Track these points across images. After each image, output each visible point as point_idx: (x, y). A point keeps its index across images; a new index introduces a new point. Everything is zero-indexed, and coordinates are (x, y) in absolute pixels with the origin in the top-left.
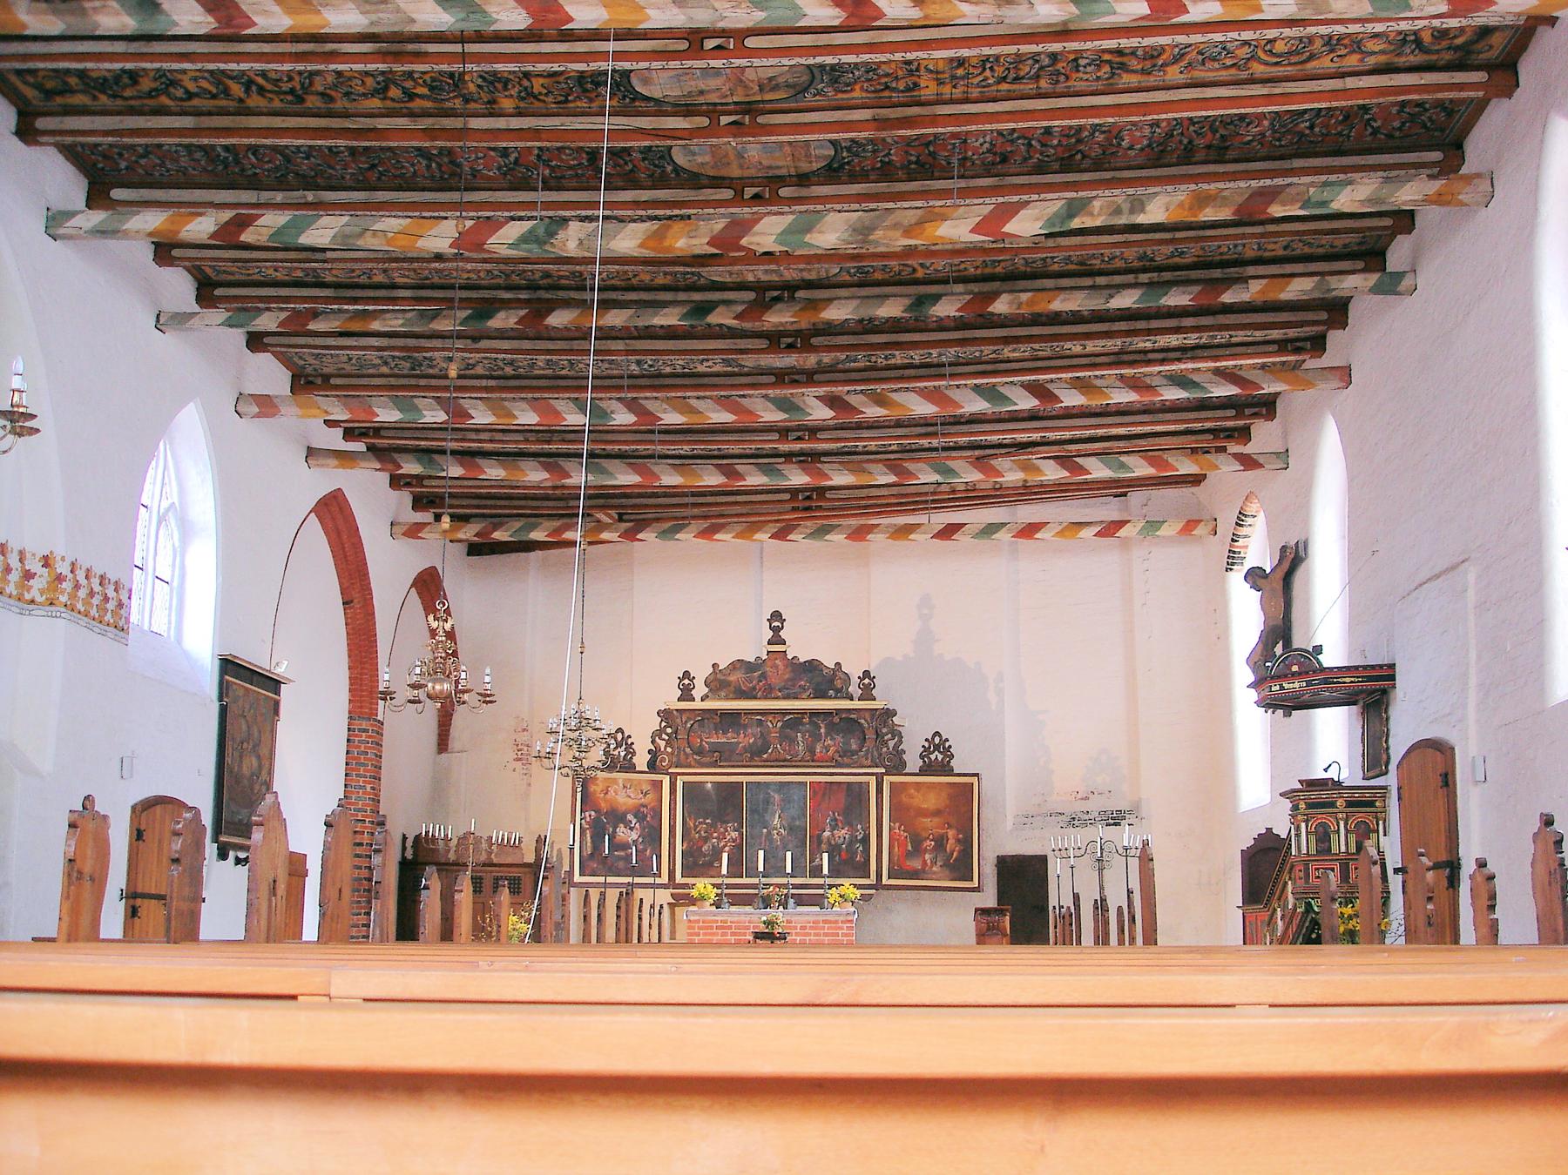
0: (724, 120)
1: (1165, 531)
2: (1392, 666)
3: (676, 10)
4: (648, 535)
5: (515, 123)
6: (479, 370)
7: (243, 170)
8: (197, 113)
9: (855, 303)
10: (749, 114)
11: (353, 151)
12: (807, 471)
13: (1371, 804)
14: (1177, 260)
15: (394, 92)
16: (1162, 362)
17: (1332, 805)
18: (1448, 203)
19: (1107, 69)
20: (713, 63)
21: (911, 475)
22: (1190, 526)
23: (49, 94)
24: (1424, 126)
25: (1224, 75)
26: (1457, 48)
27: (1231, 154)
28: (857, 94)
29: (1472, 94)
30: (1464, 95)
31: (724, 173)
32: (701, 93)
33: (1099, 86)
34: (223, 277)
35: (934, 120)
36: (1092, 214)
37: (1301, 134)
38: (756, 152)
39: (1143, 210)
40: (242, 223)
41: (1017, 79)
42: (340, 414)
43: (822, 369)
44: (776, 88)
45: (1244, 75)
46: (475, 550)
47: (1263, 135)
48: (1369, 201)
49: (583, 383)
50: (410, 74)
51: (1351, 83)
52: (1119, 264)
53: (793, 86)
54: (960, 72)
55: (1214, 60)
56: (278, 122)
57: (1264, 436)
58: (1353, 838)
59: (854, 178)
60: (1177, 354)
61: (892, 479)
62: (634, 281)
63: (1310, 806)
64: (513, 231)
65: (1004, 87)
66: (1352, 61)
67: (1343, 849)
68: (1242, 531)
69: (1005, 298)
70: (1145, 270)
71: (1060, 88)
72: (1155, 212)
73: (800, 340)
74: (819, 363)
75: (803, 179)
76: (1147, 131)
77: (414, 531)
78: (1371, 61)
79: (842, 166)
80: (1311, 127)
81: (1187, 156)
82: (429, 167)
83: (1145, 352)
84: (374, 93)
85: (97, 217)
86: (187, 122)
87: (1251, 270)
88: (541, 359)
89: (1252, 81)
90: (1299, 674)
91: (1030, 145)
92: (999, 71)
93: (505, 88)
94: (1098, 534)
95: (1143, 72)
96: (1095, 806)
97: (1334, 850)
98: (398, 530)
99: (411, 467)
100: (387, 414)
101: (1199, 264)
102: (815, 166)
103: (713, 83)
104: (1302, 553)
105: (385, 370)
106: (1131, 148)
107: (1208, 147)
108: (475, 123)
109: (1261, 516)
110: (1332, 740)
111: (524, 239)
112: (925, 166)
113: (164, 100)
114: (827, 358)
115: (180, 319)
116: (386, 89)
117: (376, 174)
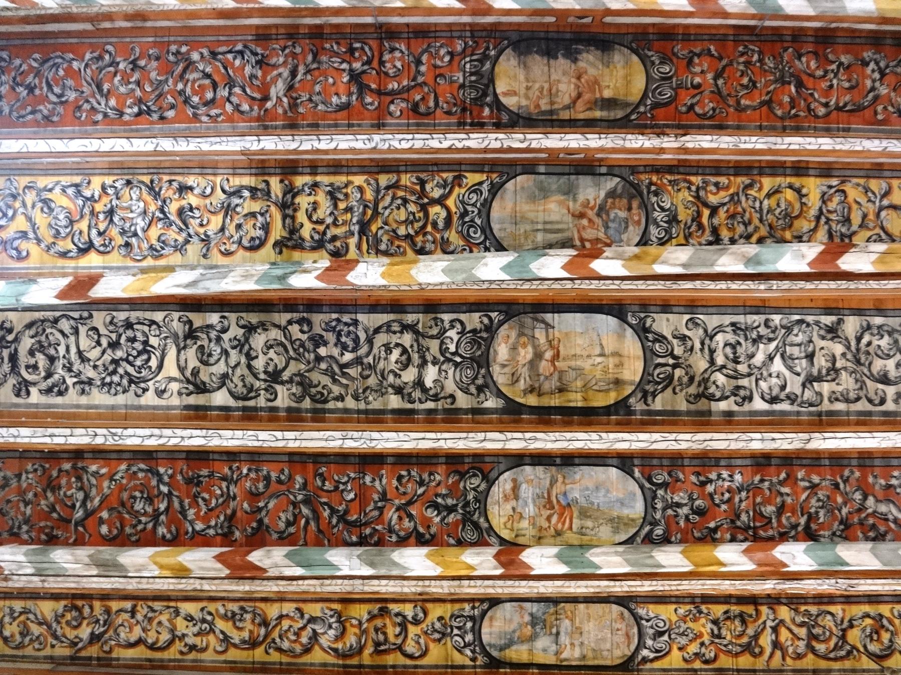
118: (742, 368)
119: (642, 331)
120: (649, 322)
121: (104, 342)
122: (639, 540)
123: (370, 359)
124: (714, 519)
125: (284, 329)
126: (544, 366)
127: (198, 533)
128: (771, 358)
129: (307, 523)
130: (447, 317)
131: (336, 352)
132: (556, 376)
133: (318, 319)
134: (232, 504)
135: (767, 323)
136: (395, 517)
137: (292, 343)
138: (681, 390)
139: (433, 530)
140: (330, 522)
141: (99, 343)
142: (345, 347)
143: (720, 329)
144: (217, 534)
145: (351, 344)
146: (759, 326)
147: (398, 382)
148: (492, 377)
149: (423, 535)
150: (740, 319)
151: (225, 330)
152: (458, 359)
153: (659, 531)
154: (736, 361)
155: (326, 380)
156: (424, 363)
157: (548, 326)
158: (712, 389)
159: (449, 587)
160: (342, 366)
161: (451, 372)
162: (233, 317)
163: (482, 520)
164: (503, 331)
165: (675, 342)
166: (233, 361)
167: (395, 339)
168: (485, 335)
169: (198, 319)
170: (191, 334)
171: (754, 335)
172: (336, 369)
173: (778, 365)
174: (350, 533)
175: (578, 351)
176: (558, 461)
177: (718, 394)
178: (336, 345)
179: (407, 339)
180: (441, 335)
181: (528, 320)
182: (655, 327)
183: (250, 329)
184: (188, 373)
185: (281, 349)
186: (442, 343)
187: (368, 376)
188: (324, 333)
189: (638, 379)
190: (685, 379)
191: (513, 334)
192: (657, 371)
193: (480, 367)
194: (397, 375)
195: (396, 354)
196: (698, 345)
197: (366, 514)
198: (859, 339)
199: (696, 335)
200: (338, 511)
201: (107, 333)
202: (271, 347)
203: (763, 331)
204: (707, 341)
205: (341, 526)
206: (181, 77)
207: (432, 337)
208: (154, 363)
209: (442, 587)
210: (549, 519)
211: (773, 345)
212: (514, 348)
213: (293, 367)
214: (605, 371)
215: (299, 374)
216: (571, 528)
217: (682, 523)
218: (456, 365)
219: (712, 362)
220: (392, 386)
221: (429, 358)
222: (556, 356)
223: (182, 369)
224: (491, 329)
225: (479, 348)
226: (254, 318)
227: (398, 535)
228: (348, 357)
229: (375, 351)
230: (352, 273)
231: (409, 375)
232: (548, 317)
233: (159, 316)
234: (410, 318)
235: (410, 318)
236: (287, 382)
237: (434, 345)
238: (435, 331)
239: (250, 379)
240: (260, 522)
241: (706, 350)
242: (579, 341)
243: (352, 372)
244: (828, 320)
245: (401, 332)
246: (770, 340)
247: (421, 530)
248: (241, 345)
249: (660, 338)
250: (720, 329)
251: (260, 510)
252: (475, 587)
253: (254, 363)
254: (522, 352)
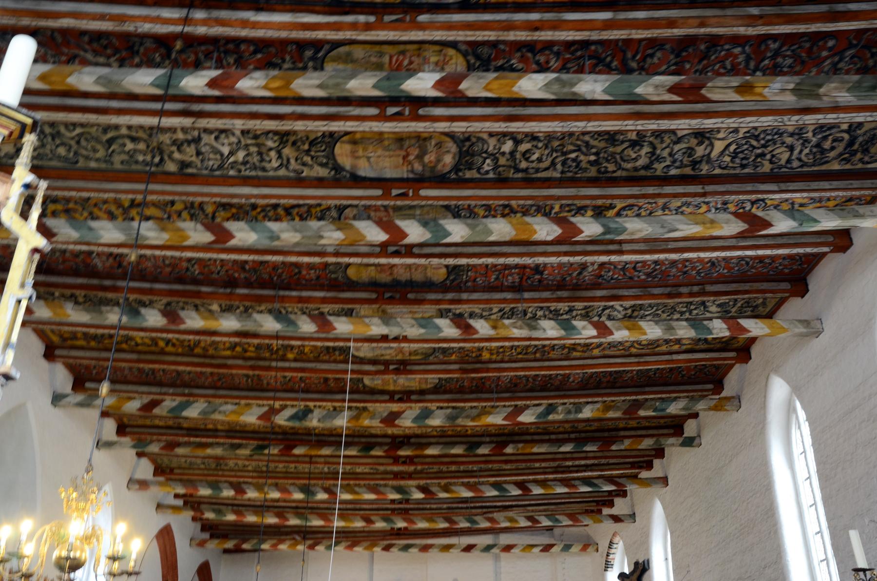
0: (391, 367)
3: (384, 327)
4: (320, 548)
5: (294, 365)
6: (250, 468)
7: (155, 377)
8: (139, 352)
9: (441, 446)
10: (403, 366)
11: (212, 374)
12: (405, 520)
14: (588, 428)
15: (238, 349)
16: (577, 472)
18: (720, 410)
19: (567, 350)
20: (392, 345)
21: (455, 523)
23: (65, 340)
24: (705, 373)
25: (618, 353)
26: (723, 342)
27: (618, 385)
28: (453, 357)
29: (729, 362)
30: (726, 362)
31: (386, 388)
32: (382, 355)
33: (563, 357)
34: (131, 423)
35: (488, 370)
36: (557, 413)
37: (650, 377)
38: (403, 382)
39: (581, 412)
40: (154, 404)
41: (526, 354)
42: (181, 490)
43: (416, 472)
44: (417, 354)
45: (627, 353)
46: (226, 551)
47: (633, 377)
48: (683, 409)
49: (342, 506)
50: (248, 343)
51: (675, 357)
52: (561, 429)
53: (426, 354)
54: (501, 350)
55: (614, 347)
56: (179, 359)
57: (620, 507)
59: (445, 392)
60: (584, 468)
61: (446, 525)
62: (334, 432)
64: (288, 412)
65: (520, 356)
66: (676, 347)
68: (612, 551)
69: (511, 446)
70: (572, 432)
71: (544, 357)
72: (587, 413)
73: (409, 460)
74: (415, 469)
75: (422, 392)
76: (581, 375)
77: (202, 544)
78: (684, 347)
79: (441, 387)
80: (655, 374)
81: (598, 386)
82: (247, 381)
83: (569, 467)
84: (228, 349)
85: (80, 397)
86: (134, 356)
87: (622, 433)
88: (281, 465)
89: (630, 355)
91: (528, 380)
92: (519, 350)
93: (292, 349)
95: (583, 351)
98: (193, 543)
99: (210, 515)
100: (205, 492)
101: (603, 433)
102: (429, 386)
103: (388, 352)
105: (202, 466)
106: (573, 382)
107: (608, 382)
108: (274, 364)
109: (621, 543)
111: (292, 418)
112: (480, 390)
113: (124, 346)
114: (419, 468)
115: (109, 445)
116: (235, 347)
117: (223, 386)
118: (253, 149)
119: (337, 168)
120: (333, 173)
121: (768, 157)
122: (327, 47)
123: (555, 155)
124: (258, 60)
125: (620, 168)
126: (415, 152)
127: (739, 45)
128: (231, 153)
129: (634, 57)
130: (491, 175)
131: (582, 157)
132: (405, 147)
133: (593, 172)
134: (700, 67)
135: (240, 171)
136: (551, 64)
137: (616, 162)
138: (301, 138)
139: (518, 55)
140: (613, 57)
141: (773, 156)
142: (574, 160)
143: (276, 169)
144: (722, 46)
145: (569, 162)
146: (246, 170)
147: (535, 143)
148: (458, 146)
149: (528, 51)
150: (260, 173)
151: (668, 166)
152: (484, 155)
153: (309, 53)
154: (260, 153)
155: (593, 142)
156: (512, 153)
157: (412, 171)
158: (276, 138)
159: (508, 36)
160: (579, 150)
161: (491, 148)
162: (658, 173)
163: (472, 61)
164: (447, 169)
165: (310, 162)
166: (668, 150)
167: (534, 165)
168: (462, 167)
169: (688, 171)
170: (695, 164)
171: (248, 166)
172: (584, 149)
173: (226, 150)
174: (595, 51)
175: (387, 159)
176: (403, 99)
177: (270, 135)
178: (581, 161)
179: (524, 165)
180: (496, 167)
181: (427, 174)
182: (328, 171)
183: (646, 167)
184: (707, 142)
185: (626, 158)
186: (496, 163)
187: (559, 146)
188: (588, 166)
189: (338, 145)
190: (299, 144)
191: (439, 167)
192: (323, 148)
193: (467, 151)
194: (536, 147)
195: (534, 157)
196: (292, 161)
197: (578, 64)
198: (162, 160)
199: (293, 164)
200: (604, 66)
201: (764, 162)
202: (633, 159)
203: (243, 168)
204: (285, 162)
205: (604, 55)
206: (656, 270)
207: (503, 166)
208: (733, 147)
209: (515, 36)
210: (411, 63)
211: (232, 160)
212: (438, 161)
213: (619, 149)
214: (365, 150)
215: (615, 146)
216: (391, 57)
217: (288, 58)
218: (486, 152)
219: (279, 153)
220: (540, 141)
221: (508, 156)
222: (404, 158)
223: (712, 145)
224: (456, 168)
225: (466, 161)
226: (643, 173)
227: (551, 51)
228: (573, 155)
229: (550, 159)
230: (557, 234)
231: (524, 147)
232: (411, 176)
233: (717, 171)
234: (520, 175)
235: (520, 175)
236: (626, 141)
237: (502, 161)
238: (501, 169)
239: (657, 142)
240: (677, 56)
241: (285, 158)
242: (387, 164)
243: (571, 148)
244: (190, 170)
245: (527, 169)
246: (235, 162)
247: (530, 55)
248: (659, 159)
249: (322, 165)
250: (276, 169)
251: (674, 64)
252: (484, 36)
253: (649, 150)
254: (433, 158)
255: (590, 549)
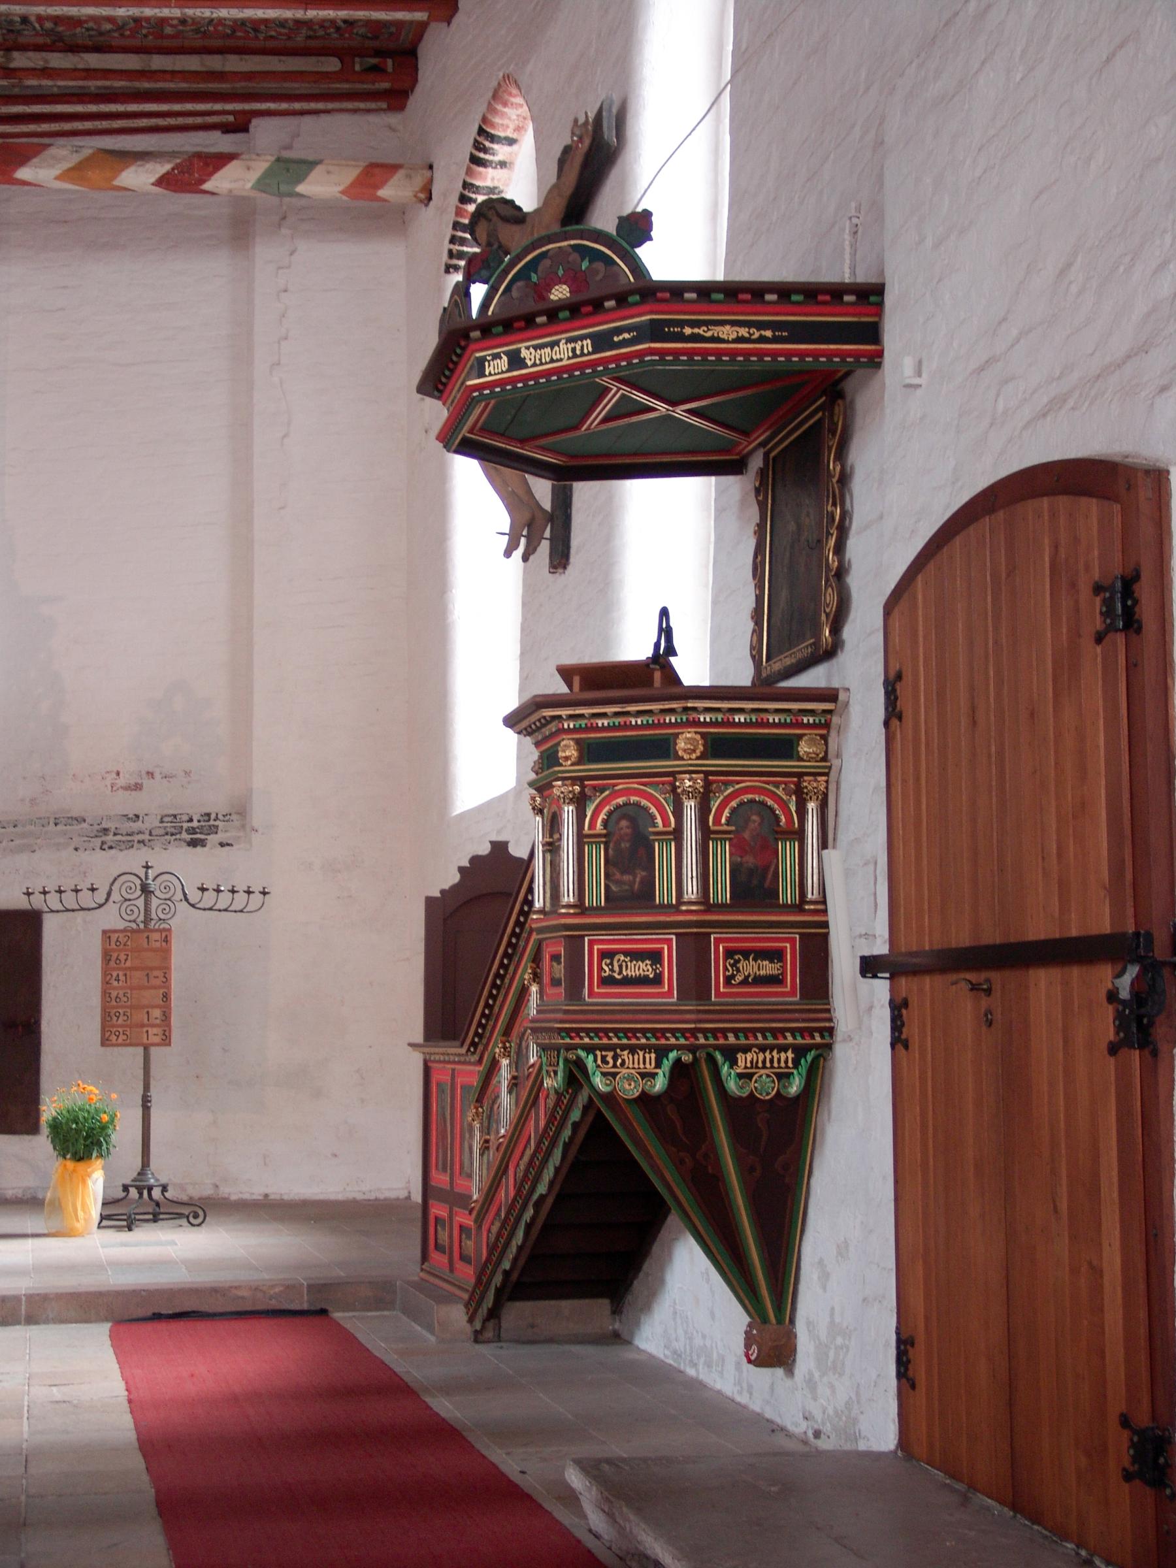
1: (323, 186)
2: (871, 295)
13: (784, 747)
17: (662, 748)
22: (375, 173)
58: (723, 857)
63: (591, 752)
67: (691, 890)
90: (575, 310)
94: (161, 182)
96: (154, 802)
97: (664, 893)
104: (609, 134)
110: (672, 559)
255: (393, 191)
